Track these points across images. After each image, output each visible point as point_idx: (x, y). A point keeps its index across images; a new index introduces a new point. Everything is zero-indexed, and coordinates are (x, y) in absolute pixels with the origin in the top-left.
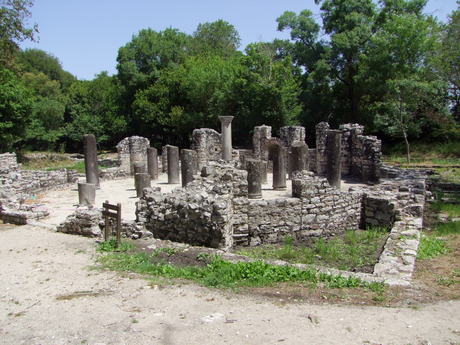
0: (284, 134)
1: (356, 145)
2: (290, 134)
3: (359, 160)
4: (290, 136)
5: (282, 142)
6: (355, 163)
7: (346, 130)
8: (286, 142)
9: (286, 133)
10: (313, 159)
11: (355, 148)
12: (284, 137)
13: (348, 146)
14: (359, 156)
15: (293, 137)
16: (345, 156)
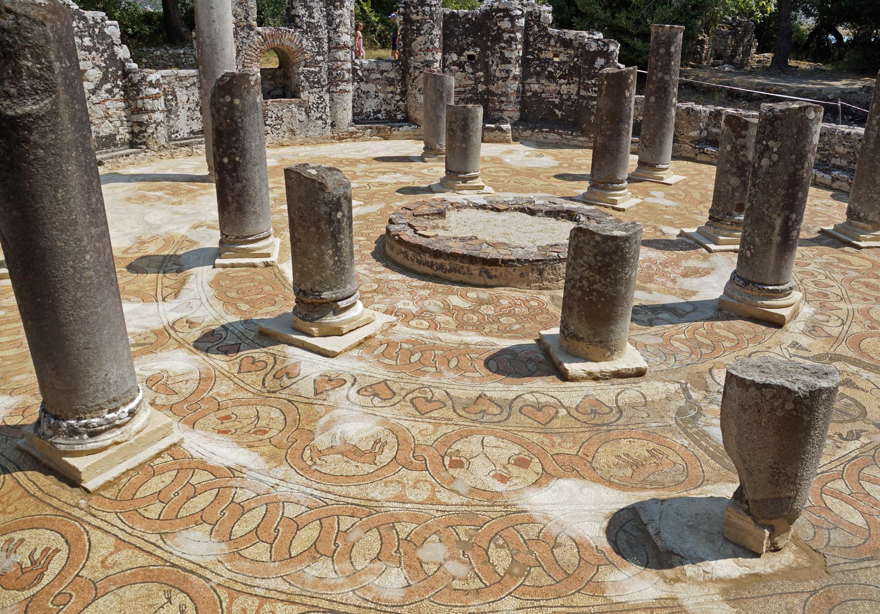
0: (311, 16)
1: (540, 50)
2: (328, 15)
3: (553, 86)
4: (329, 23)
5: (304, 42)
6: (535, 94)
7: (519, 13)
8: (317, 39)
9: (316, 15)
10: (391, 89)
11: (539, 59)
12: (309, 24)
13: (521, 54)
14: (551, 77)
15: (338, 26)
16: (515, 78)
